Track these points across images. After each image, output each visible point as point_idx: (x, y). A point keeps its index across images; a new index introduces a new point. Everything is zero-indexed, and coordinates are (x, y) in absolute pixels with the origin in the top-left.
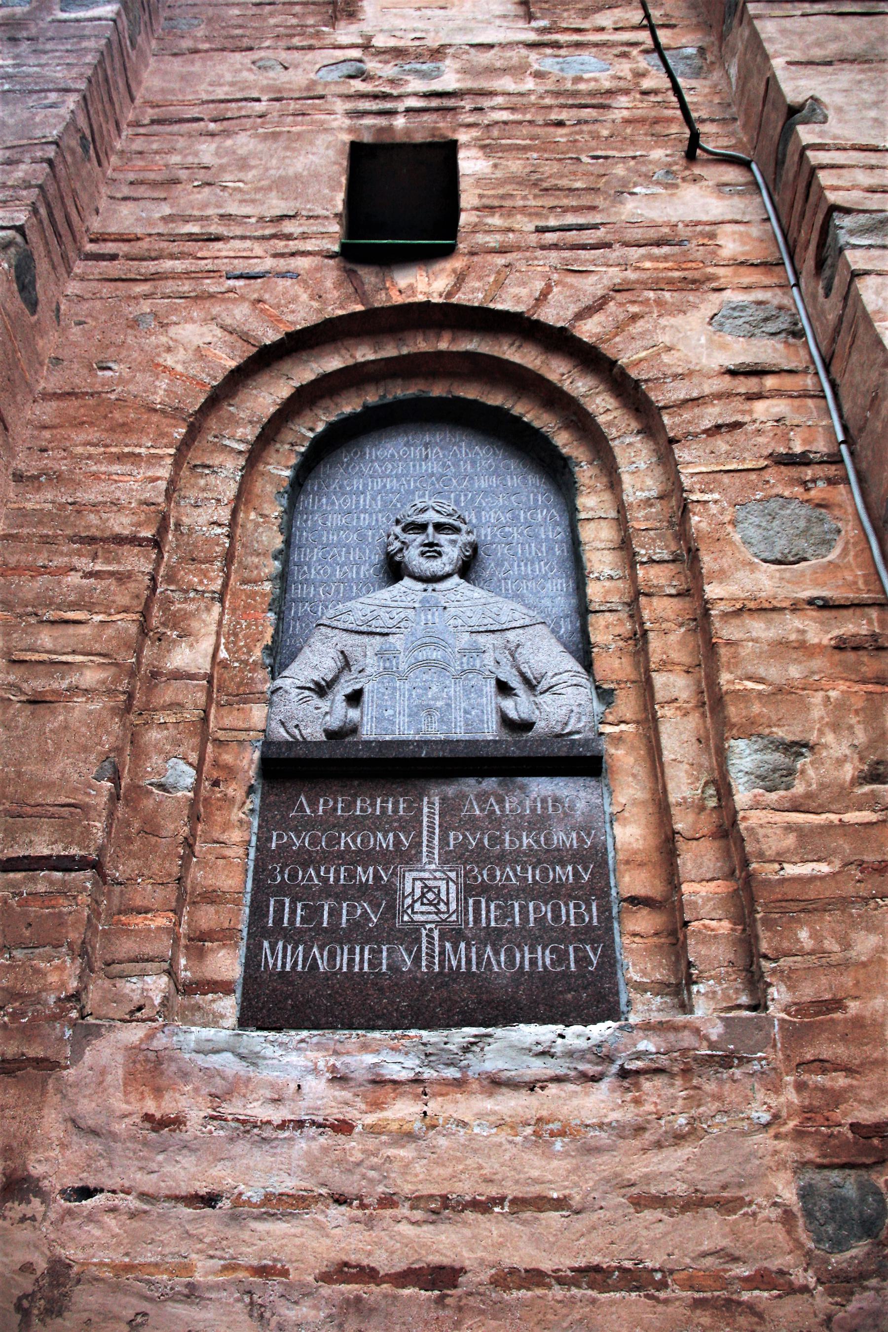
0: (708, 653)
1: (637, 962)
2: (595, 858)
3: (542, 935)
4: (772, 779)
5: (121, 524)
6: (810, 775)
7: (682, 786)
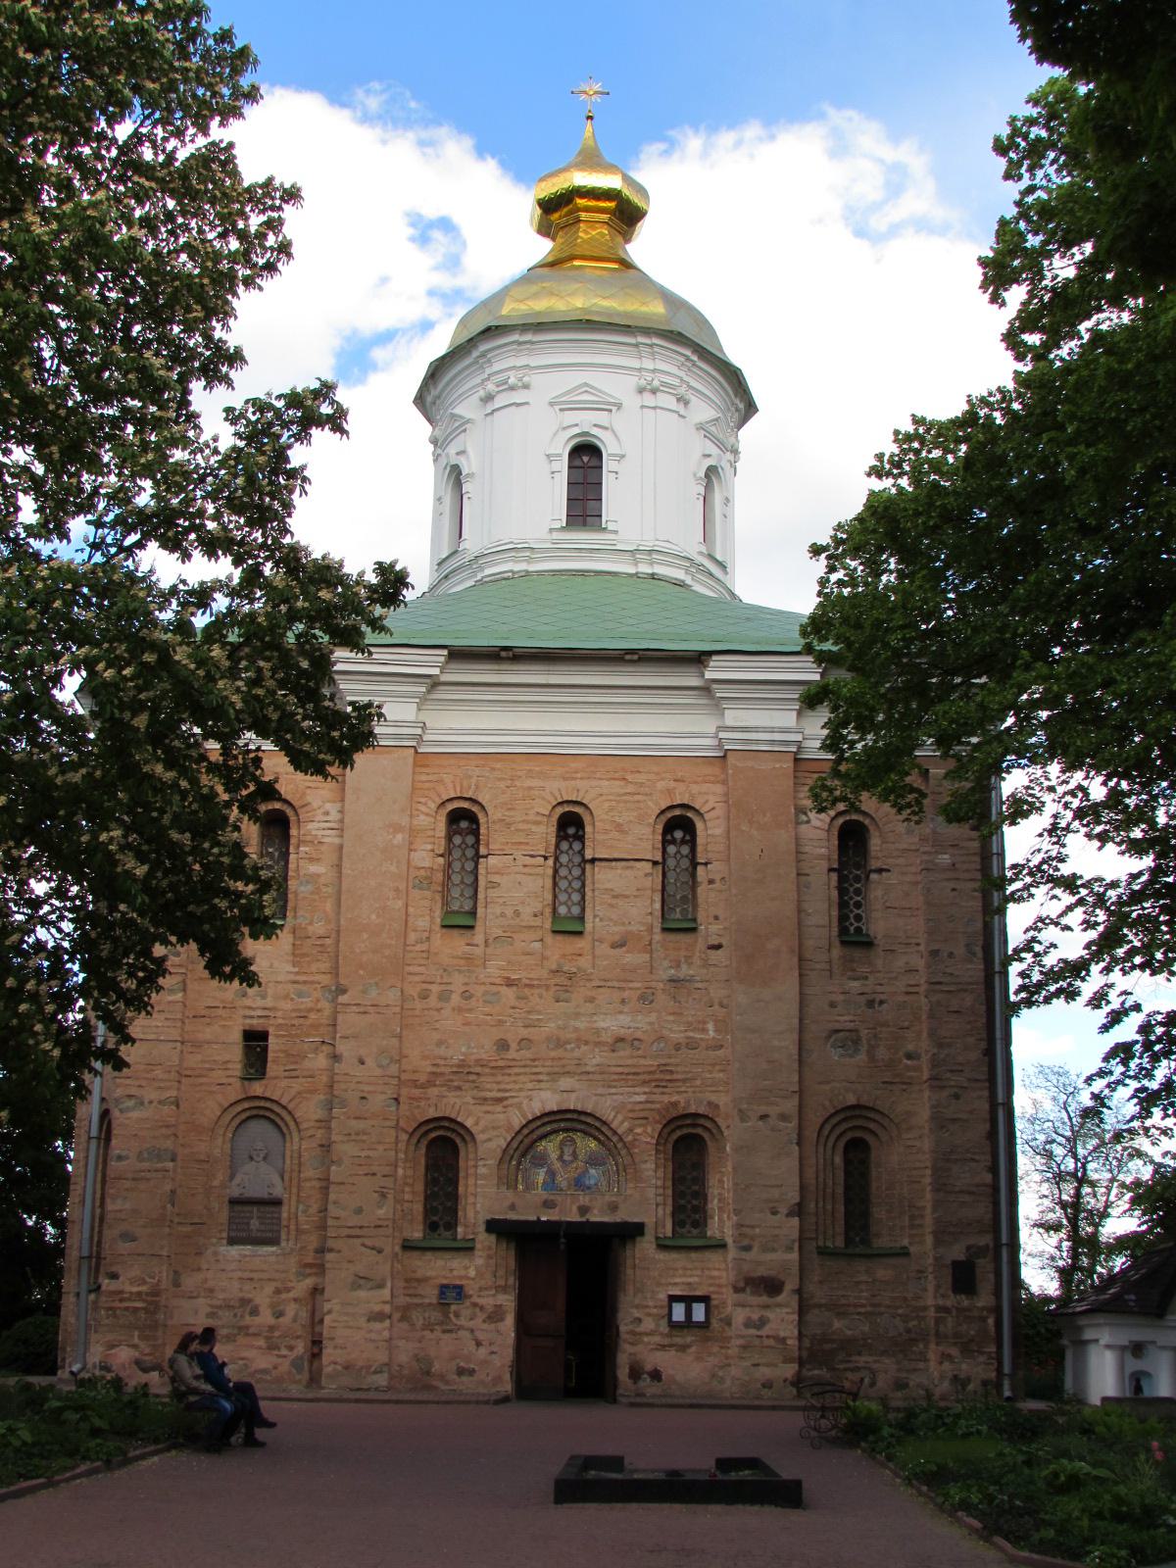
0: (299, 1188)
1: (283, 1236)
2: (279, 1219)
4: (304, 1212)
5: (202, 1157)
6: (312, 1211)
7: (293, 1210)
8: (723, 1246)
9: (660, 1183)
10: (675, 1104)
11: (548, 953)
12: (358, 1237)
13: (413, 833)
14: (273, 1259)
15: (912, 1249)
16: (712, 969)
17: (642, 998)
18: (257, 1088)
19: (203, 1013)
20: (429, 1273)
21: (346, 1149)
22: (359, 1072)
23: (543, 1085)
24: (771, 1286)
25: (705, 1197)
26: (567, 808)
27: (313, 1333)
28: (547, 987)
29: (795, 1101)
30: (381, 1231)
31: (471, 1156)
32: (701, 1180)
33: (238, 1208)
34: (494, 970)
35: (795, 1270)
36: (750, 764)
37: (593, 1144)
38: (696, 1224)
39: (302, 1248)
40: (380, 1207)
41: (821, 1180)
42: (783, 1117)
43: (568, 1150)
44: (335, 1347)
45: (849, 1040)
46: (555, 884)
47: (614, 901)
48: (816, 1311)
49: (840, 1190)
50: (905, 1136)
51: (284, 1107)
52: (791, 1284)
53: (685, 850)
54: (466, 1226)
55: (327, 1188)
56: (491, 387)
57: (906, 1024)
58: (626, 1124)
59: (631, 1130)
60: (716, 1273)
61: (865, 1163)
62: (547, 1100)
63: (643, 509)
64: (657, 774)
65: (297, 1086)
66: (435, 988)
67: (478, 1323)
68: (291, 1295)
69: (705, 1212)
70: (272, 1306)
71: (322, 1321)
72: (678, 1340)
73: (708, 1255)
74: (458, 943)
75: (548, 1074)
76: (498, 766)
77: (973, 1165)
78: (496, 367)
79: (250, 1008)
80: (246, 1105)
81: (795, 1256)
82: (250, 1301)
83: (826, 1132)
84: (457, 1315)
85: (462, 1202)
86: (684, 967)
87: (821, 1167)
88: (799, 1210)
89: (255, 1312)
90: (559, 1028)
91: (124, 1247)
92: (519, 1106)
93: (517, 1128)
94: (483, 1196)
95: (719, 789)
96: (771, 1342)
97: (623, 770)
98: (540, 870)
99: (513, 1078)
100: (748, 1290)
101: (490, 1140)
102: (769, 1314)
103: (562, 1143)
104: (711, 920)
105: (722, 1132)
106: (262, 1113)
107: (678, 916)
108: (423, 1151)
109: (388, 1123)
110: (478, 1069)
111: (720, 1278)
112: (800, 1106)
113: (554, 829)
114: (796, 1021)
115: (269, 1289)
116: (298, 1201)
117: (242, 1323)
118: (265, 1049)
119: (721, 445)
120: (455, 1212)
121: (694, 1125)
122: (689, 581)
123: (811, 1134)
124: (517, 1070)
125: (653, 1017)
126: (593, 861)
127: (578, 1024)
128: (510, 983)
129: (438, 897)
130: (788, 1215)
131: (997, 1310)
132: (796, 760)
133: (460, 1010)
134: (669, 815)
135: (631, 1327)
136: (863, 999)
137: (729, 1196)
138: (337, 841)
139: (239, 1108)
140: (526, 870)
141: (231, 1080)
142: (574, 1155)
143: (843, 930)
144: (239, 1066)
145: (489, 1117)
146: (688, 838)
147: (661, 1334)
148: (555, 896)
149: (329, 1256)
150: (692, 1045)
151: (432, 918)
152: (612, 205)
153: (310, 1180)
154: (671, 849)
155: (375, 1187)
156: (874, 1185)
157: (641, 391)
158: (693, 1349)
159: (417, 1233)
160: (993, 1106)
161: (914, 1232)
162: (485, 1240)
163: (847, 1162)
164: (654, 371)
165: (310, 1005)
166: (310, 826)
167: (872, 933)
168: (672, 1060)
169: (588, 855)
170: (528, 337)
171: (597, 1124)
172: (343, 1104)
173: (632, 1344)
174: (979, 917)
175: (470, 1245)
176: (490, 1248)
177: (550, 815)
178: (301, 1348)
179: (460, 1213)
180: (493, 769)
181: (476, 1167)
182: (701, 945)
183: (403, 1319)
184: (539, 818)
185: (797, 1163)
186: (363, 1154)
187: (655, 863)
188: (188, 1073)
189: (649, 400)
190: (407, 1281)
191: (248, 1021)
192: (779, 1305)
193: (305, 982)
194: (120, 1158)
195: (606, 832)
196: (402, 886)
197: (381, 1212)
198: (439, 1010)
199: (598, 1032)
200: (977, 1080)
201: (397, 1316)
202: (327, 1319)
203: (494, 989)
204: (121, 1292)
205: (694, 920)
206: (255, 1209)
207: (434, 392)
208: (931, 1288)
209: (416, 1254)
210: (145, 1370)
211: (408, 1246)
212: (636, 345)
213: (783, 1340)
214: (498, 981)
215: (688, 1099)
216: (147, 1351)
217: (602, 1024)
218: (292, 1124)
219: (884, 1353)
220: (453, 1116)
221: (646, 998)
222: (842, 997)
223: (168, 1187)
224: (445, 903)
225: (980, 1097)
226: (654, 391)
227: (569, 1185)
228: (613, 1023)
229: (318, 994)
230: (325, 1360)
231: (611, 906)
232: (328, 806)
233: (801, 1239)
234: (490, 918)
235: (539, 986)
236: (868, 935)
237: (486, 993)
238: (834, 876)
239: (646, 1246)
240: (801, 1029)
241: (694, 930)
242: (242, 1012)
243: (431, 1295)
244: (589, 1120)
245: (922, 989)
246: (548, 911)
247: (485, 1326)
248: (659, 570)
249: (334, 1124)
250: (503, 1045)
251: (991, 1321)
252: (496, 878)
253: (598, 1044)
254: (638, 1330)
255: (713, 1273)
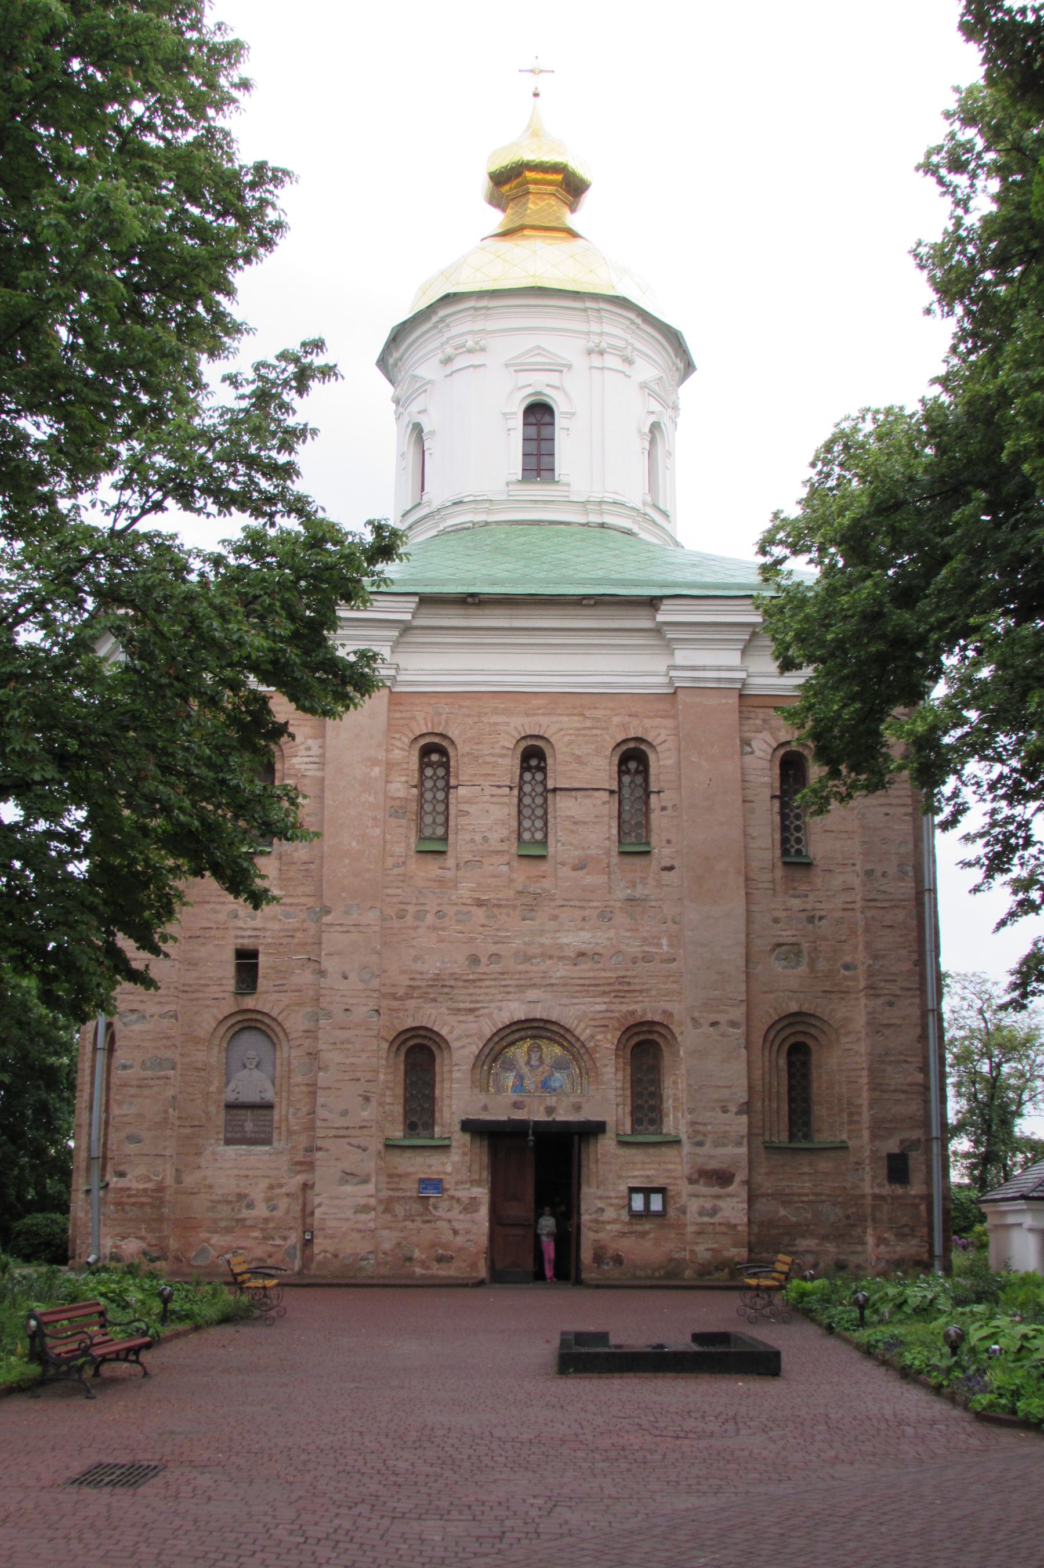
0: (289, 1092)
1: (275, 1136)
2: (272, 1121)
3: (263, 1132)
4: (295, 1114)
5: (200, 1065)
6: (300, 1113)
8: (678, 1142)
9: (619, 1085)
10: (633, 1013)
11: (515, 876)
12: (344, 1137)
13: (390, 766)
14: (266, 1157)
15: (850, 1143)
16: (666, 889)
17: (602, 916)
18: (249, 1002)
19: (198, 933)
20: (410, 1170)
21: (332, 1057)
22: (342, 985)
23: (510, 997)
24: (722, 1178)
25: (660, 1097)
26: (530, 742)
27: (304, 1224)
28: (515, 907)
29: (743, 1008)
30: (365, 1132)
31: (446, 1062)
32: (657, 1082)
33: (235, 1112)
34: (465, 890)
35: (744, 1164)
36: (698, 700)
37: (557, 1050)
38: (652, 1122)
39: (293, 1147)
40: (364, 1110)
41: (767, 1081)
42: (733, 1024)
43: (535, 1056)
44: (325, 1237)
45: (789, 952)
46: (520, 812)
47: (574, 828)
48: (764, 1200)
49: (784, 1089)
50: (844, 1040)
51: (274, 1019)
52: (741, 1176)
53: (639, 779)
54: (443, 1126)
55: (315, 1093)
56: (449, 350)
57: (843, 938)
58: (588, 1031)
59: (592, 1037)
60: (671, 1167)
61: (806, 1064)
62: (516, 1010)
63: (593, 462)
64: (613, 710)
65: (286, 999)
66: (411, 909)
67: (455, 1214)
68: (283, 1190)
69: (661, 1111)
70: (268, 1200)
71: (312, 1213)
72: (639, 1228)
73: (664, 1150)
74: (432, 868)
75: (517, 986)
76: (467, 703)
77: (905, 1066)
78: (455, 331)
79: (242, 928)
80: (239, 1018)
81: (744, 1150)
82: (246, 1196)
83: (771, 1037)
84: (436, 1208)
85: (438, 1104)
86: (639, 887)
87: (767, 1069)
88: (746, 1109)
89: (250, 1206)
90: (525, 944)
91: (131, 1148)
92: (490, 1016)
93: (489, 1036)
94: (459, 1098)
95: (670, 723)
96: (724, 1229)
97: (582, 706)
98: (506, 800)
99: (483, 991)
100: (702, 1182)
101: (463, 1047)
102: (721, 1203)
103: (529, 1050)
104: (664, 844)
105: (675, 1038)
106: (253, 1024)
107: (634, 838)
108: (402, 1058)
109: (370, 1033)
110: (452, 983)
111: (675, 1170)
112: (748, 1016)
113: (518, 761)
114: (743, 936)
115: (264, 1184)
116: (289, 1105)
117: (240, 1216)
118: (256, 966)
119: (664, 403)
120: (433, 1112)
121: (651, 1032)
122: (636, 530)
123: (758, 1039)
124: (487, 983)
125: (612, 933)
126: (555, 790)
127: (542, 940)
128: (480, 903)
129: (413, 825)
130: (737, 1114)
131: (928, 1198)
132: (741, 696)
133: (434, 928)
134: (624, 748)
135: (594, 1216)
136: (803, 915)
137: (684, 1097)
138: (319, 774)
139: (233, 1021)
140: (495, 799)
141: (226, 995)
142: (541, 1060)
143: (785, 852)
144: (233, 982)
145: (464, 1026)
146: (641, 768)
147: (623, 1223)
148: (520, 824)
149: (319, 1155)
150: (647, 958)
151: (408, 844)
152: (559, 177)
153: (298, 1085)
154: (626, 779)
155: (358, 1090)
156: (815, 1085)
157: (590, 352)
158: (652, 1236)
159: (397, 1132)
160: (924, 1015)
161: (853, 1127)
162: (460, 1140)
163: (790, 1064)
164: (601, 334)
165: (296, 925)
166: (294, 760)
167: (811, 855)
168: (629, 973)
169: (550, 785)
170: (484, 303)
171: (562, 1032)
172: (329, 1015)
173: (596, 1232)
174: (911, 839)
175: (446, 1142)
176: (465, 1146)
177: (514, 749)
178: (294, 1238)
179: (437, 1114)
180: (461, 707)
181: (451, 1072)
182: (654, 866)
183: (386, 1210)
184: (505, 752)
185: (744, 1066)
186: (348, 1061)
187: (612, 792)
188: (186, 988)
189: (596, 360)
190: (390, 1176)
191: (240, 941)
192: (730, 1195)
193: (291, 904)
194: (125, 1067)
195: (567, 763)
196: (380, 815)
197: (365, 1114)
198: (415, 928)
199: (561, 947)
200: (910, 989)
201: (381, 1208)
202: (318, 1212)
203: (465, 909)
204: (129, 1189)
205: (648, 843)
206: (249, 1112)
207: (396, 355)
208: (867, 1178)
209: (397, 1151)
210: (153, 1260)
211: (390, 1146)
212: (585, 310)
213: (735, 1226)
214: (469, 901)
215: (647, 1008)
216: (153, 1242)
217: (565, 940)
218: (281, 1035)
219: (825, 1238)
220: (429, 1026)
221: (606, 916)
222: (784, 914)
223: (170, 1092)
224: (420, 831)
225: (911, 1004)
226: (601, 353)
227: (536, 1090)
228: (574, 940)
229: (303, 915)
230: (316, 1250)
231: (572, 832)
232: (310, 742)
233: (750, 1135)
234: (461, 844)
235: (506, 906)
236: (807, 856)
237: (457, 913)
238: (777, 803)
239: (607, 1144)
240: (748, 945)
241: (647, 853)
242: (234, 933)
243: (411, 1188)
244: (554, 1028)
245: (859, 905)
246: (515, 836)
247: (461, 1217)
248: (608, 519)
249: (320, 1034)
250: (474, 960)
251: (923, 1207)
252: (465, 807)
253: (561, 958)
254: (601, 1219)
255: (671, 1168)
